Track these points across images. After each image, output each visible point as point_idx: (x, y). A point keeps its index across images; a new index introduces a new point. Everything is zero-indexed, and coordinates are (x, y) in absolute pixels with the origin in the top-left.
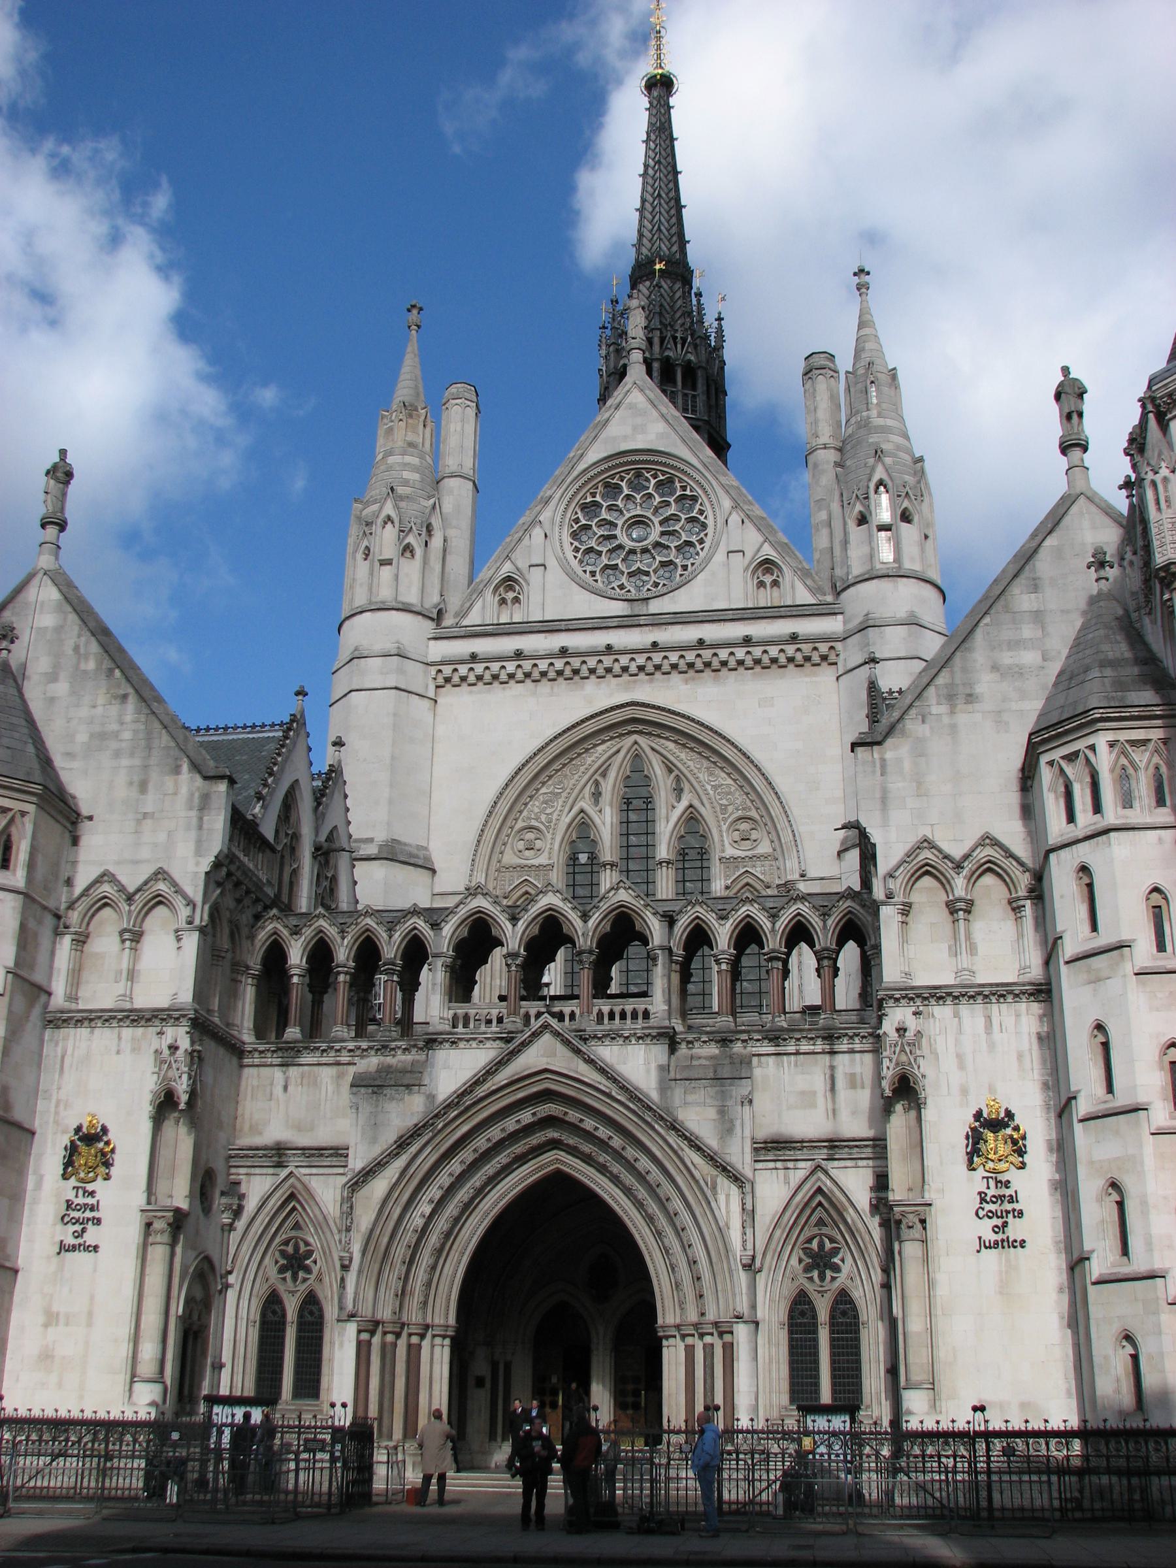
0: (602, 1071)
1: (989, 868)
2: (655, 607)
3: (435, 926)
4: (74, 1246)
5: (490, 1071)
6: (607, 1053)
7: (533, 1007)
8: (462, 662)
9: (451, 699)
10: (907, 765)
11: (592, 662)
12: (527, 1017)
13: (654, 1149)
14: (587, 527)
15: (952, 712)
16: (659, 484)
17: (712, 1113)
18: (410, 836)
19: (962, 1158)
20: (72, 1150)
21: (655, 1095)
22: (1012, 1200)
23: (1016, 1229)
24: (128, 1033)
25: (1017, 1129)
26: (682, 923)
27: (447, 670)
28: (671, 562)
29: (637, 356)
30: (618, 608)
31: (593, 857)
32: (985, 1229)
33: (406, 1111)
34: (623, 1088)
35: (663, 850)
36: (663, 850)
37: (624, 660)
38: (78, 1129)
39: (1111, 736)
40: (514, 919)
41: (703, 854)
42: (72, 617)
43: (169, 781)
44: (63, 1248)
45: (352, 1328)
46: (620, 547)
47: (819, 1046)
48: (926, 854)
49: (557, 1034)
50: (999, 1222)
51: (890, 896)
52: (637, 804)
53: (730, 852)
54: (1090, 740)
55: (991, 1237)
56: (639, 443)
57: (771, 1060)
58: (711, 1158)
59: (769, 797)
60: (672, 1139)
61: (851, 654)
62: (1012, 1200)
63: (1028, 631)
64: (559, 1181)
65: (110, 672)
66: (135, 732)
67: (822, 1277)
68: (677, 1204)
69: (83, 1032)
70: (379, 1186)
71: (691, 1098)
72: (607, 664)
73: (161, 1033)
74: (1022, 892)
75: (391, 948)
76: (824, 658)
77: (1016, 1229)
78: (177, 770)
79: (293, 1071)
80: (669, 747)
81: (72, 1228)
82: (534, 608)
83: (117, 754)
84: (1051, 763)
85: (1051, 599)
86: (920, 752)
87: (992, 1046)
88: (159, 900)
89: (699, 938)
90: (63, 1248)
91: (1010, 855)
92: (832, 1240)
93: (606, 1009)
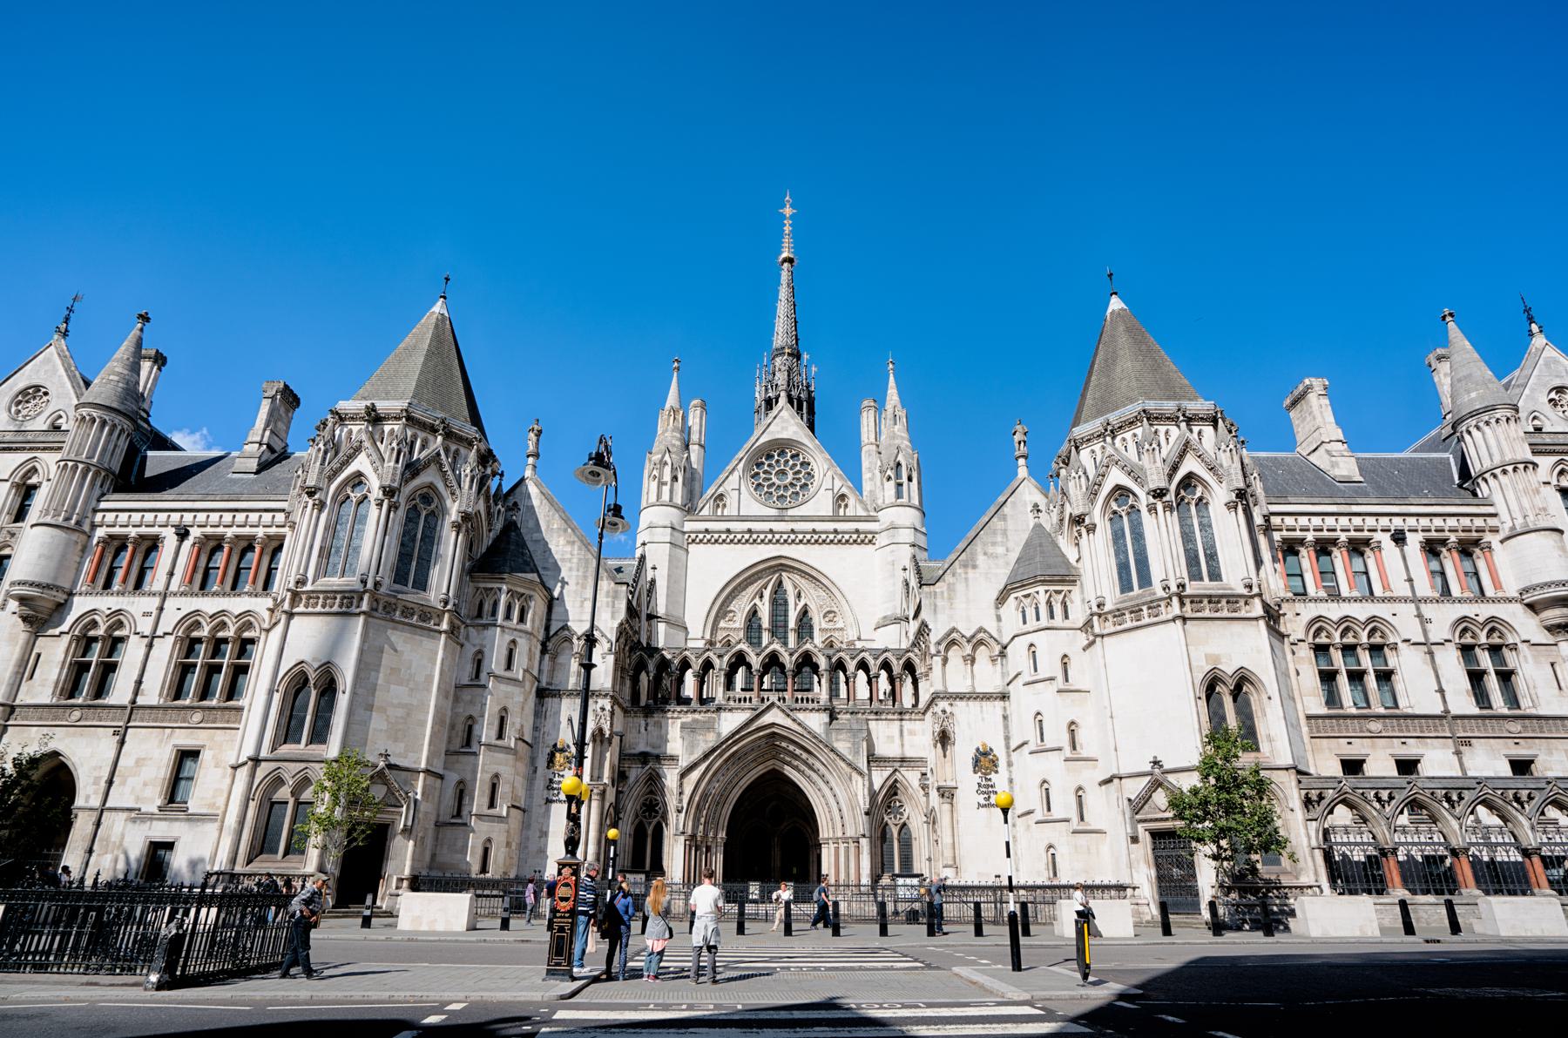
1: (981, 642)
2: (790, 512)
3: (720, 656)
7: (765, 695)
9: (692, 548)
18: (677, 613)
29: (783, 394)
30: (774, 512)
31: (760, 626)
33: (707, 741)
35: (792, 624)
36: (792, 624)
41: (811, 627)
48: (954, 635)
52: (779, 603)
53: (824, 625)
61: (881, 540)
63: (999, 539)
72: (772, 538)
75: (696, 664)
80: (797, 578)
82: (731, 510)
86: (951, 588)
89: (840, 666)
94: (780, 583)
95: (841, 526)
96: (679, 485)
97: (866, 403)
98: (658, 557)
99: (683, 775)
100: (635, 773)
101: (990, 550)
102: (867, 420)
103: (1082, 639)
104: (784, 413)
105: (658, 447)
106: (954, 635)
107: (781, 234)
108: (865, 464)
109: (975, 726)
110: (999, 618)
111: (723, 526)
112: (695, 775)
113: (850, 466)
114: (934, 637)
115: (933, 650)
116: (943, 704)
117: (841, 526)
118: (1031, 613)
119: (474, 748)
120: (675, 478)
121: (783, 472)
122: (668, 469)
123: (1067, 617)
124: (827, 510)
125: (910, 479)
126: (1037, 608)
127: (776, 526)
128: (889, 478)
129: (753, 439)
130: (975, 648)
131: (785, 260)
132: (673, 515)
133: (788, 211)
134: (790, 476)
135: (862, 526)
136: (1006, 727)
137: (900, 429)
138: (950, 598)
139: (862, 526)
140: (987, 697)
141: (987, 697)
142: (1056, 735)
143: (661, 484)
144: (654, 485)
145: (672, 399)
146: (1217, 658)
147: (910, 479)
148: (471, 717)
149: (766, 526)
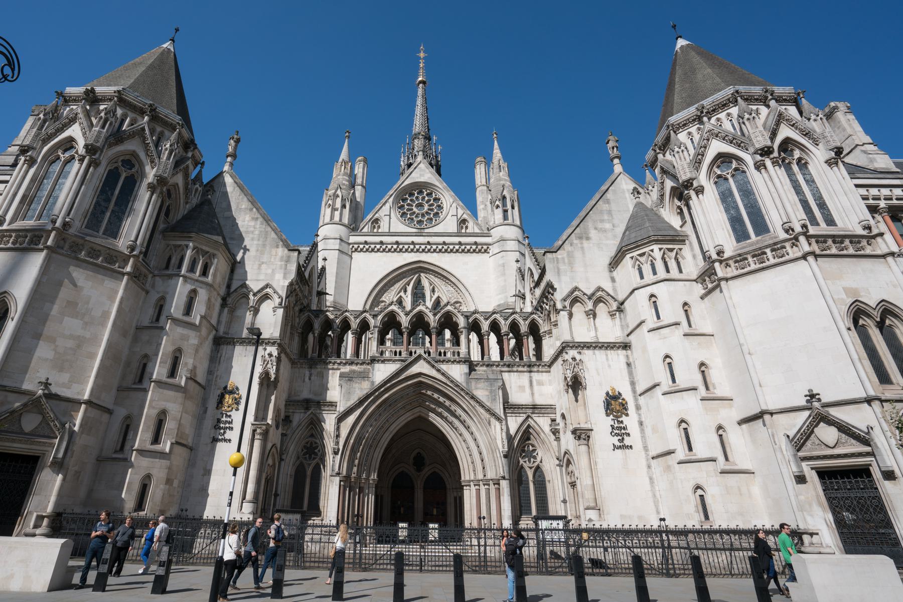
0: (443, 374)
1: (599, 300)
2: (426, 231)
8: (361, 243)
9: (355, 255)
10: (566, 260)
11: (406, 247)
12: (411, 354)
13: (464, 406)
14: (403, 206)
15: (582, 243)
16: (427, 195)
17: (487, 393)
21: (464, 384)
22: (624, 429)
23: (627, 441)
25: (623, 399)
26: (470, 320)
27: (356, 246)
28: (431, 219)
30: (415, 230)
32: (615, 440)
34: (452, 382)
37: (417, 247)
39: (660, 246)
40: (407, 314)
46: (414, 213)
47: (525, 369)
49: (425, 359)
50: (619, 437)
51: (565, 307)
52: (419, 295)
54: (651, 248)
55: (618, 444)
56: (422, 179)
57: (506, 376)
58: (488, 410)
59: (467, 294)
60: (472, 402)
61: (494, 249)
62: (624, 429)
63: (606, 217)
67: (530, 461)
68: (473, 429)
71: (479, 386)
72: (413, 248)
74: (615, 308)
76: (485, 251)
77: (627, 441)
80: (432, 277)
84: (632, 258)
85: (613, 207)
86: (570, 255)
87: (609, 366)
91: (609, 295)
92: (533, 446)
93: (442, 351)
94: (419, 282)
95: (464, 240)
96: (346, 211)
97: (478, 159)
98: (328, 256)
99: (341, 419)
100: (298, 417)
101: (600, 225)
102: (480, 171)
103: (699, 289)
104: (422, 165)
105: (333, 185)
106: (577, 293)
107: (418, 68)
108: (479, 198)
109: (603, 373)
110: (613, 280)
111: (377, 239)
112: (351, 419)
113: (468, 199)
114: (558, 296)
115: (559, 306)
116: (572, 353)
117: (464, 240)
118: (647, 269)
120: (344, 206)
121: (420, 205)
122: (339, 201)
123: (681, 271)
125: (513, 207)
126: (653, 265)
127: (417, 239)
128: (498, 207)
129: (400, 182)
130: (596, 304)
131: (420, 82)
132: (341, 231)
133: (422, 55)
134: (426, 207)
136: (631, 373)
137: (504, 175)
138: (571, 264)
142: (687, 375)
143: (334, 209)
144: (329, 211)
145: (344, 155)
146: (855, 291)
147: (513, 207)
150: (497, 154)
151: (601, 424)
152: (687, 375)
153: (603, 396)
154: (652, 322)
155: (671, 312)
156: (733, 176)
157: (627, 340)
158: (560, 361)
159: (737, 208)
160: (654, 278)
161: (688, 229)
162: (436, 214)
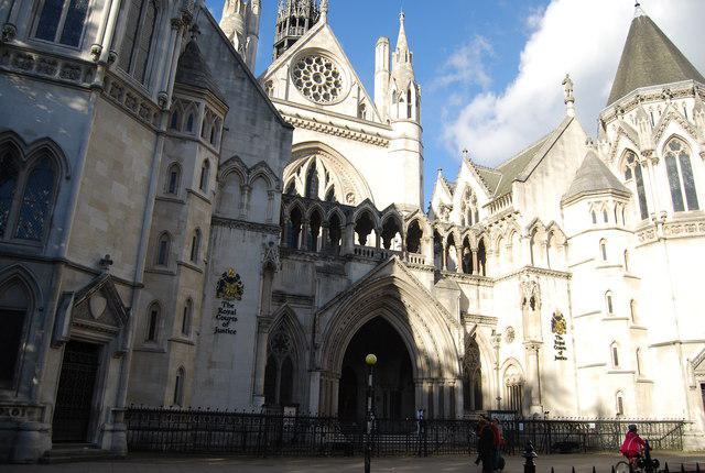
2: (325, 108)
4: (223, 331)
5: (371, 274)
6: (414, 273)
19: (550, 327)
20: (221, 284)
23: (565, 354)
24: (248, 233)
30: (313, 105)
32: (556, 352)
33: (338, 285)
38: (225, 274)
42: (215, 34)
43: (266, 123)
44: (217, 331)
45: (318, 374)
47: (475, 282)
55: (558, 356)
63: (561, 157)
64: (379, 320)
65: (236, 66)
66: (250, 97)
68: (434, 334)
69: (226, 229)
70: (329, 314)
73: (264, 236)
77: (565, 354)
78: (270, 120)
79: (284, 261)
81: (221, 322)
83: (240, 104)
86: (534, 189)
88: (261, 175)
90: (217, 331)
94: (313, 165)
97: (382, 40)
101: (556, 164)
102: (381, 53)
103: (635, 240)
109: (553, 297)
110: (562, 216)
116: (533, 277)
118: (600, 217)
119: (173, 267)
121: (317, 78)
124: (354, 113)
128: (402, 100)
135: (381, 132)
138: (533, 194)
139: (381, 132)
140: (558, 274)
141: (558, 274)
148: (166, 233)
149: (311, 115)
150: (402, 37)
151: (549, 338)
152: (621, 309)
153: (551, 317)
154: (600, 261)
155: (615, 257)
156: (680, 157)
157: (571, 271)
158: (515, 281)
159: (679, 185)
160: (604, 225)
161: (632, 186)
162: (334, 92)
